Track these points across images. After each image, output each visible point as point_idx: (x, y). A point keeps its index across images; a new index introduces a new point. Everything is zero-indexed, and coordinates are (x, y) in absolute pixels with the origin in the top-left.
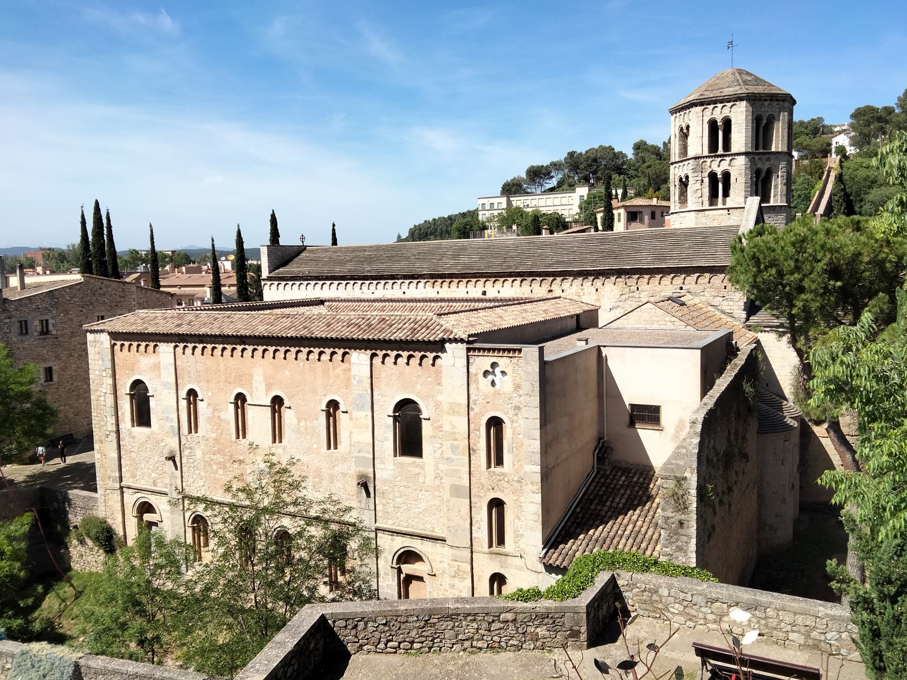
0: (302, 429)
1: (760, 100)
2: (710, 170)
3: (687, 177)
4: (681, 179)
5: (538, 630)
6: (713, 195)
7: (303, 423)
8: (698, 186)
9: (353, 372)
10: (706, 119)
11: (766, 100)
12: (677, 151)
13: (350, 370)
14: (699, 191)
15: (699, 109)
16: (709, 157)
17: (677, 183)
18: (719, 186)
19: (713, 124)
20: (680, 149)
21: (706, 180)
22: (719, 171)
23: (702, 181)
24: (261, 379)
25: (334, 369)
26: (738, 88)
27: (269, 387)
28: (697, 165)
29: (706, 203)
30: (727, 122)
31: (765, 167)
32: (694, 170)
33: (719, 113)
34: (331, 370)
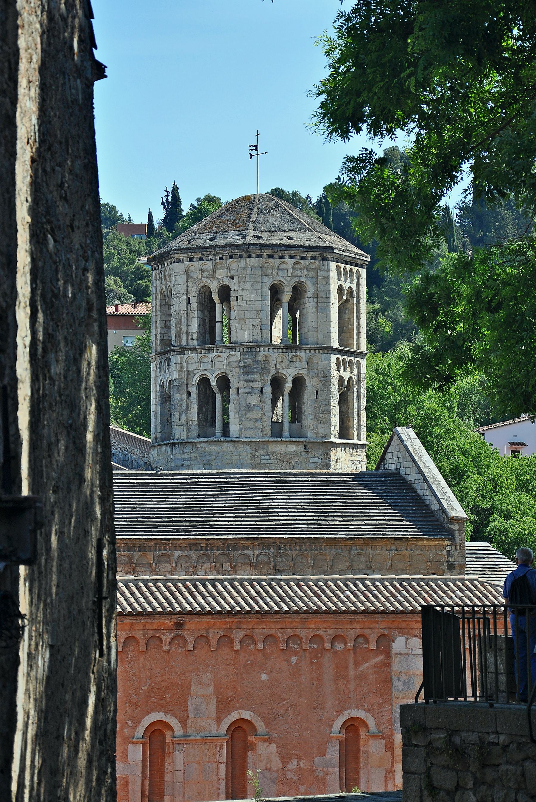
0: (289, 775)
2: (273, 372)
4: (204, 382)
7: (293, 765)
8: (254, 399)
9: (396, 667)
10: (268, 282)
12: (194, 328)
13: (389, 665)
15: (253, 261)
17: (194, 390)
19: (275, 292)
20: (202, 325)
21: (268, 390)
22: (289, 374)
24: (210, 690)
25: (357, 664)
27: (224, 706)
34: (351, 665)
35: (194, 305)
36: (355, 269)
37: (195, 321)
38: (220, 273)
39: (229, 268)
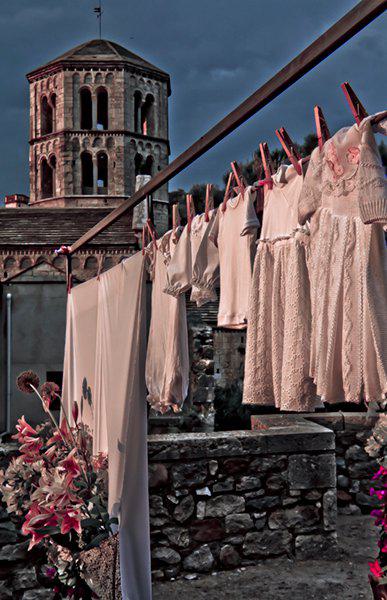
1: (139, 72)
2: (82, 150)
3: (53, 159)
4: (44, 160)
5: (224, 509)
6: (87, 182)
10: (78, 87)
11: (144, 76)
14: (70, 175)
16: (82, 133)
18: (91, 171)
21: (79, 163)
23: (74, 162)
26: (112, 56)
28: (67, 142)
29: (79, 190)
30: (103, 95)
31: (146, 155)
32: (64, 148)
33: (92, 81)
35: (39, 111)
36: (154, 82)
37: (39, 122)
38: (51, 85)
39: (54, 81)
